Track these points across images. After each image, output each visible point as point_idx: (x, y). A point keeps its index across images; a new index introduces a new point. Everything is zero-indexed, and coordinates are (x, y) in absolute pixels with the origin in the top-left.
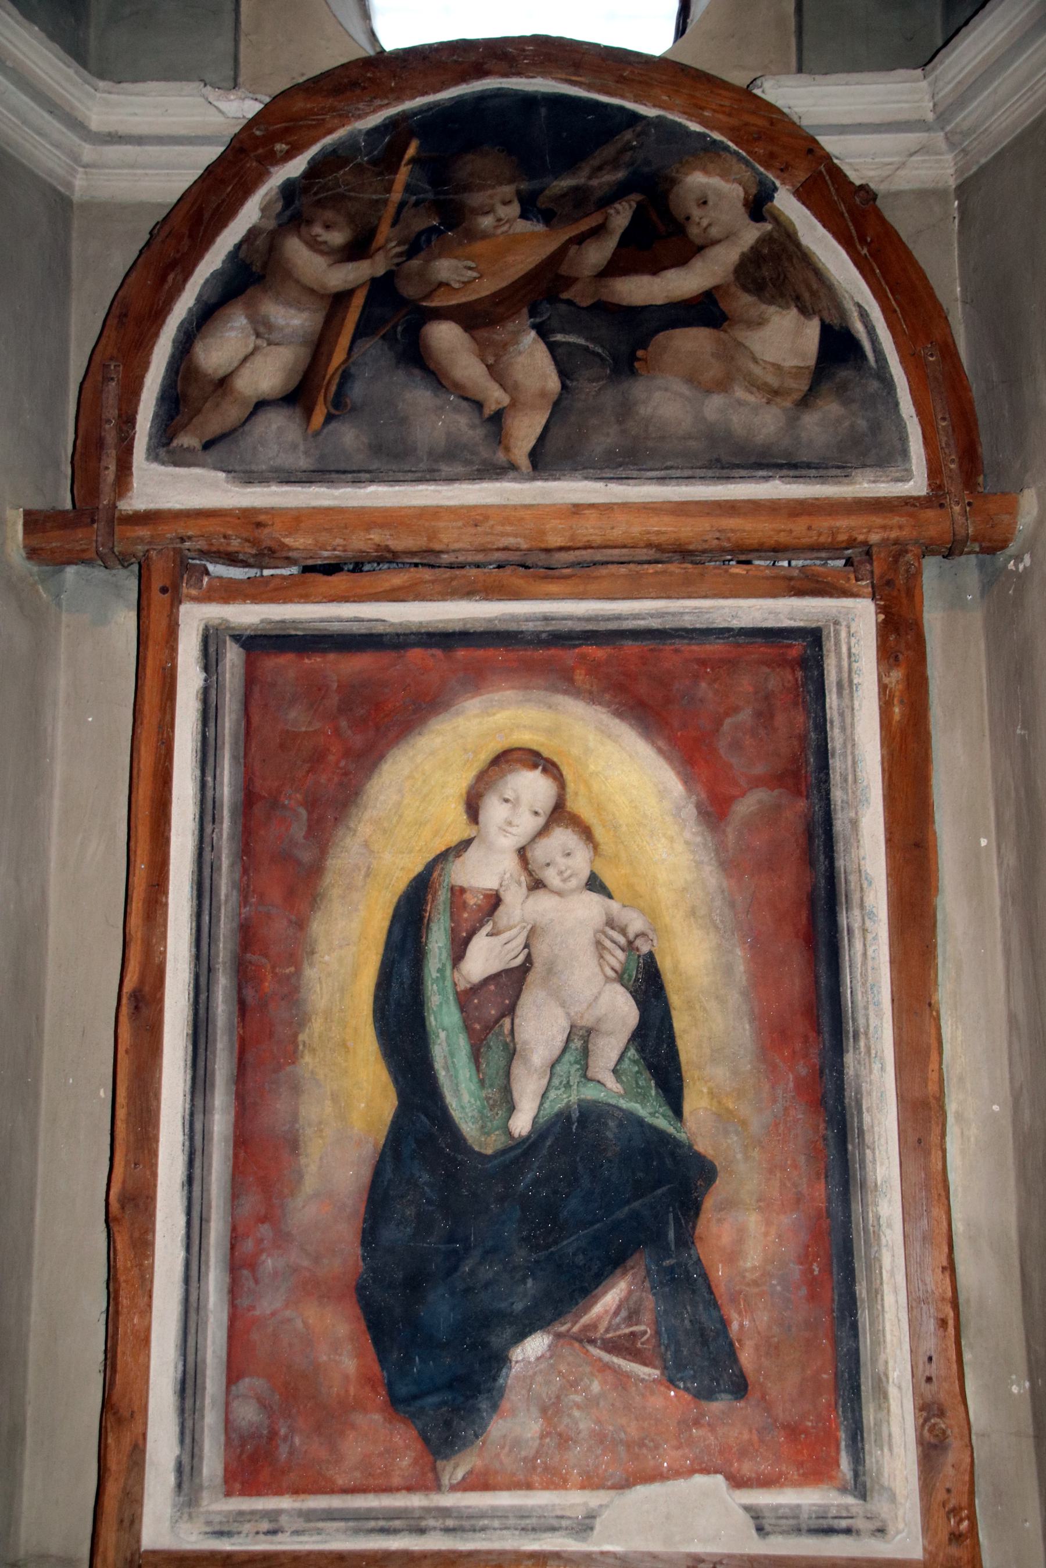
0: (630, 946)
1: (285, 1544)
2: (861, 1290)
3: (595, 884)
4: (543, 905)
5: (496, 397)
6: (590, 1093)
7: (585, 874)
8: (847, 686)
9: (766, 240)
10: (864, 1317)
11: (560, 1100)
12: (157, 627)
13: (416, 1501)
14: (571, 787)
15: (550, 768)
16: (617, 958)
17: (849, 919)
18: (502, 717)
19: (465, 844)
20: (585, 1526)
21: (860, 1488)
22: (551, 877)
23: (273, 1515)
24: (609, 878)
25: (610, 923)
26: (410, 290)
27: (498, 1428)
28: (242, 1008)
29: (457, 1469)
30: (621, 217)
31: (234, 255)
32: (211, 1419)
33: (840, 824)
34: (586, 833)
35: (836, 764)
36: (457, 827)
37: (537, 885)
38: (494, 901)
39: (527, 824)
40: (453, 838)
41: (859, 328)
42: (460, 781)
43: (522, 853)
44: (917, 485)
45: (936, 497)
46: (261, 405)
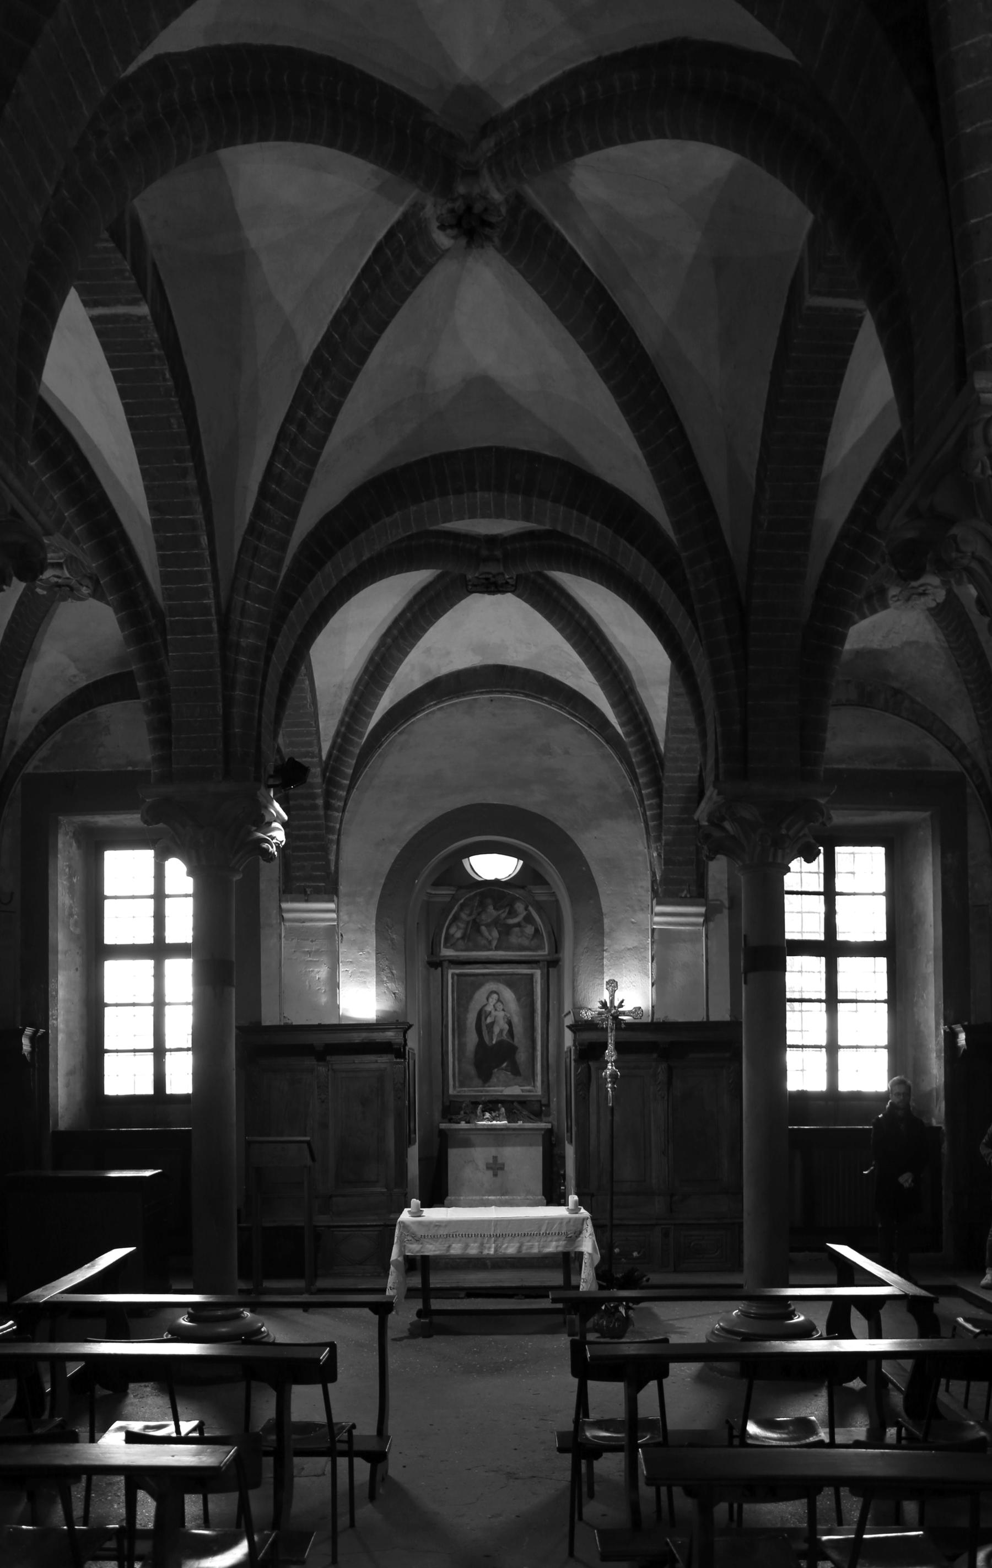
0: (508, 1019)
1: (466, 1094)
2: (535, 1063)
3: (503, 1010)
4: (497, 1013)
5: (490, 938)
6: (502, 1038)
7: (501, 1009)
8: (536, 982)
9: (527, 914)
10: (535, 1067)
11: (499, 1039)
12: (445, 973)
13: (482, 1089)
14: (501, 996)
15: (498, 994)
16: (506, 1020)
17: (536, 1015)
18: (491, 986)
19: (486, 1005)
20: (502, 1091)
21: (534, 1087)
22: (498, 1009)
23: (465, 1090)
24: (505, 1010)
25: (505, 1015)
26: (478, 920)
27: (491, 1080)
28: (459, 1026)
29: (486, 1085)
30: (507, 910)
31: (454, 915)
32: (457, 1079)
33: (535, 1002)
34: (502, 1003)
35: (535, 993)
36: (485, 1002)
37: (496, 1010)
38: (490, 1012)
39: (495, 1001)
40: (485, 1003)
41: (540, 928)
42: (486, 996)
43: (494, 1006)
44: (546, 953)
45: (549, 954)
46: (458, 939)
